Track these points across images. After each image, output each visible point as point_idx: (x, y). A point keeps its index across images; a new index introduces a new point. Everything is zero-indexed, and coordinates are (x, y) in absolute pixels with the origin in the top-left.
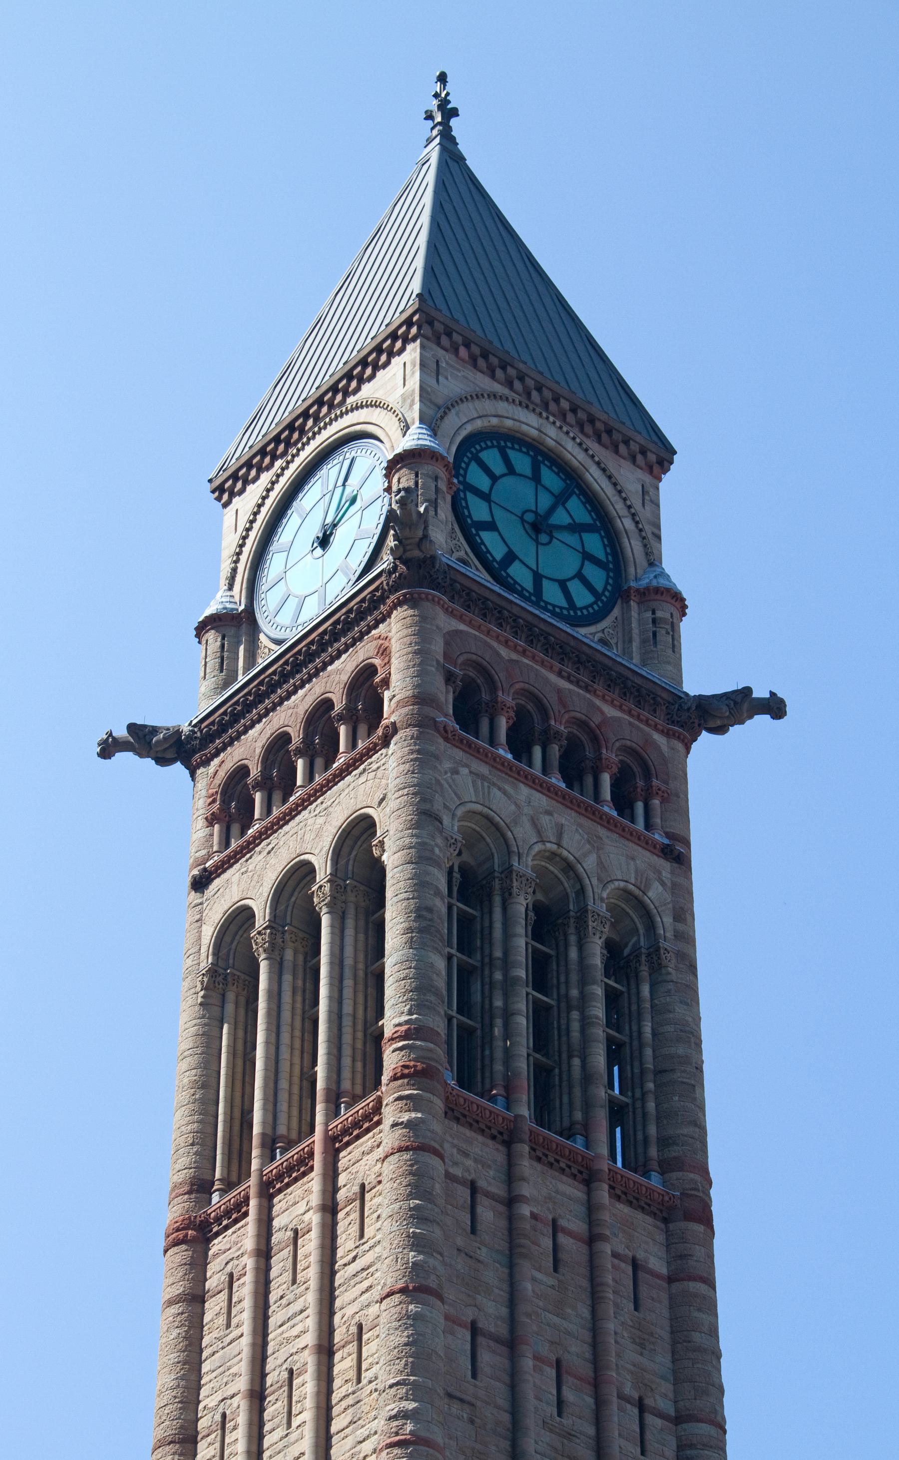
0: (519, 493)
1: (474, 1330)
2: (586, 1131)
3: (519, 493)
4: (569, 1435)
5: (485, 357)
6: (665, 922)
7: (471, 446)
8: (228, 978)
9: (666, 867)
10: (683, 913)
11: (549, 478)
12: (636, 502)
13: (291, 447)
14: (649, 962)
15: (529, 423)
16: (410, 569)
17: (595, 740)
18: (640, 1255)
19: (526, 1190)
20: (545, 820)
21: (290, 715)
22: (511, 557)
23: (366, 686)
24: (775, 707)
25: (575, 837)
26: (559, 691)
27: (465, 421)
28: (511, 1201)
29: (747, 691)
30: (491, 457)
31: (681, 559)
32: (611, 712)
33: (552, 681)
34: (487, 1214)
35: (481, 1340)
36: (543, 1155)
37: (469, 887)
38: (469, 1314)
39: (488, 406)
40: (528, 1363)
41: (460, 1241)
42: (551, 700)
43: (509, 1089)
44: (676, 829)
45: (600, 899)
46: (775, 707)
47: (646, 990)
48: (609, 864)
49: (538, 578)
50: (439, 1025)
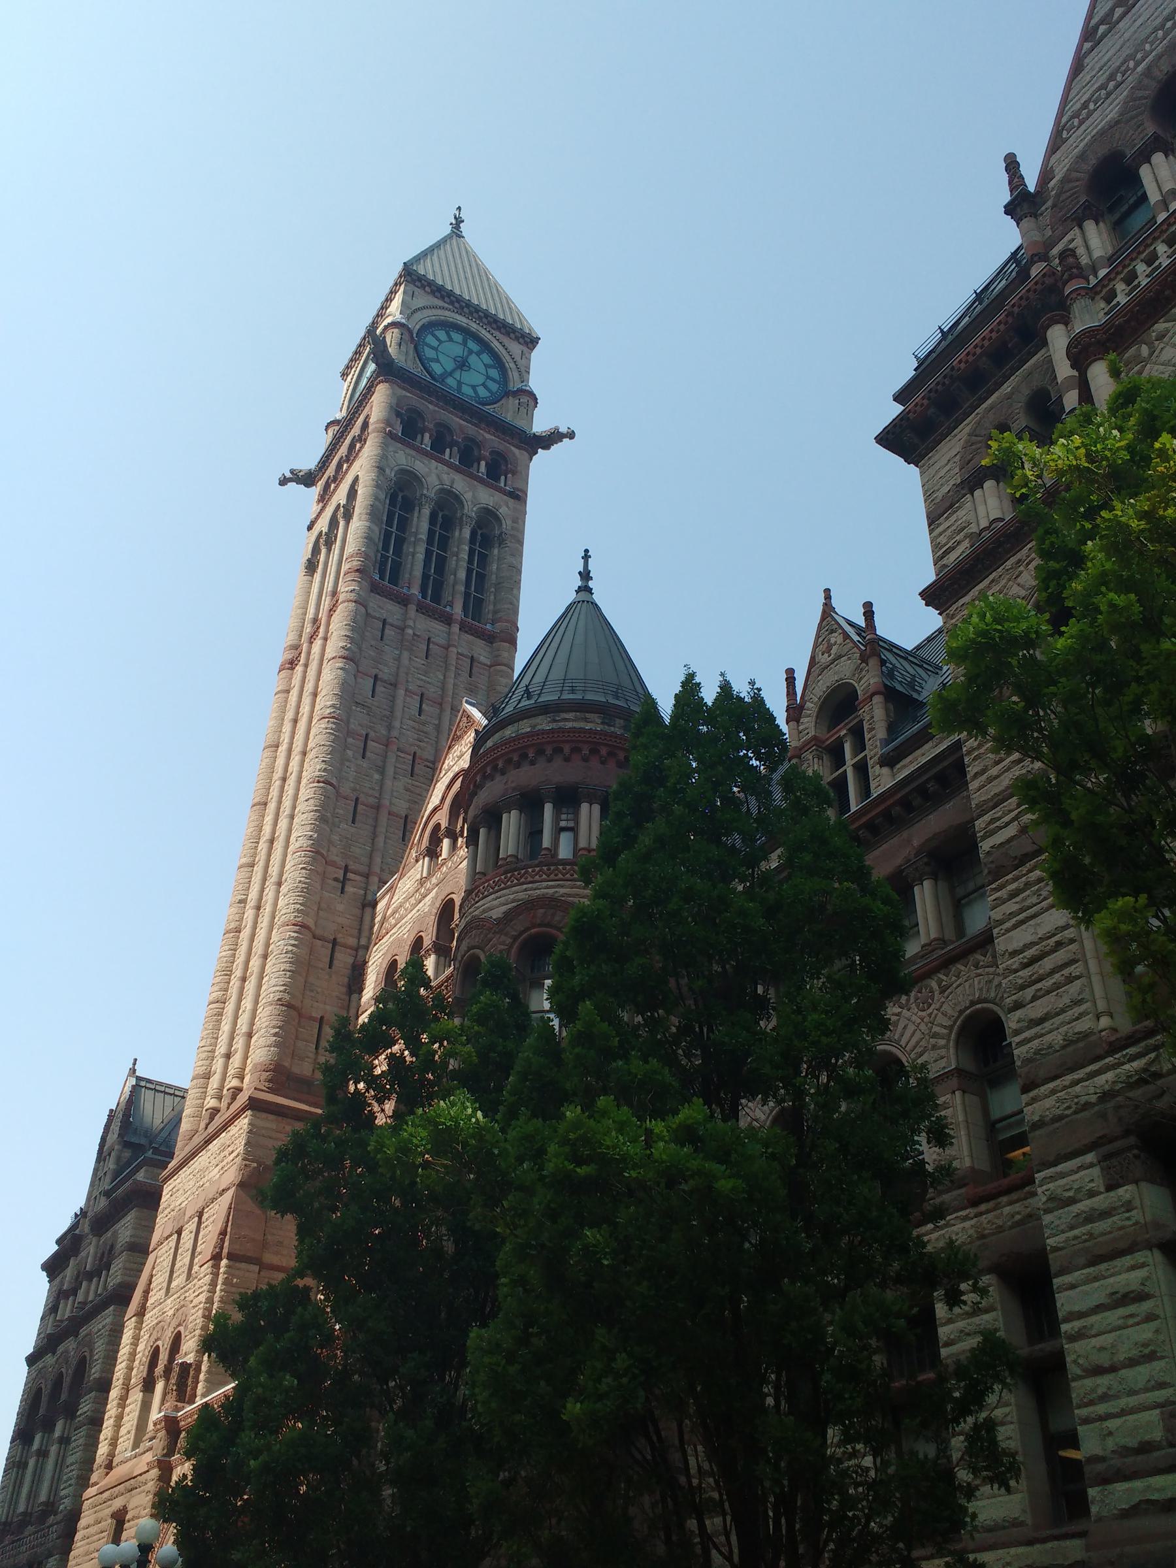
1: (376, 678)
4: (424, 724)
6: (507, 524)
9: (511, 502)
18: (475, 655)
20: (445, 477)
25: (460, 484)
26: (461, 425)
29: (557, 429)
31: (536, 382)
32: (488, 436)
34: (389, 632)
35: (379, 683)
36: (421, 609)
38: (374, 671)
40: (401, 692)
41: (373, 643)
44: (518, 485)
45: (470, 510)
47: (496, 551)
48: (476, 496)
50: (372, 555)
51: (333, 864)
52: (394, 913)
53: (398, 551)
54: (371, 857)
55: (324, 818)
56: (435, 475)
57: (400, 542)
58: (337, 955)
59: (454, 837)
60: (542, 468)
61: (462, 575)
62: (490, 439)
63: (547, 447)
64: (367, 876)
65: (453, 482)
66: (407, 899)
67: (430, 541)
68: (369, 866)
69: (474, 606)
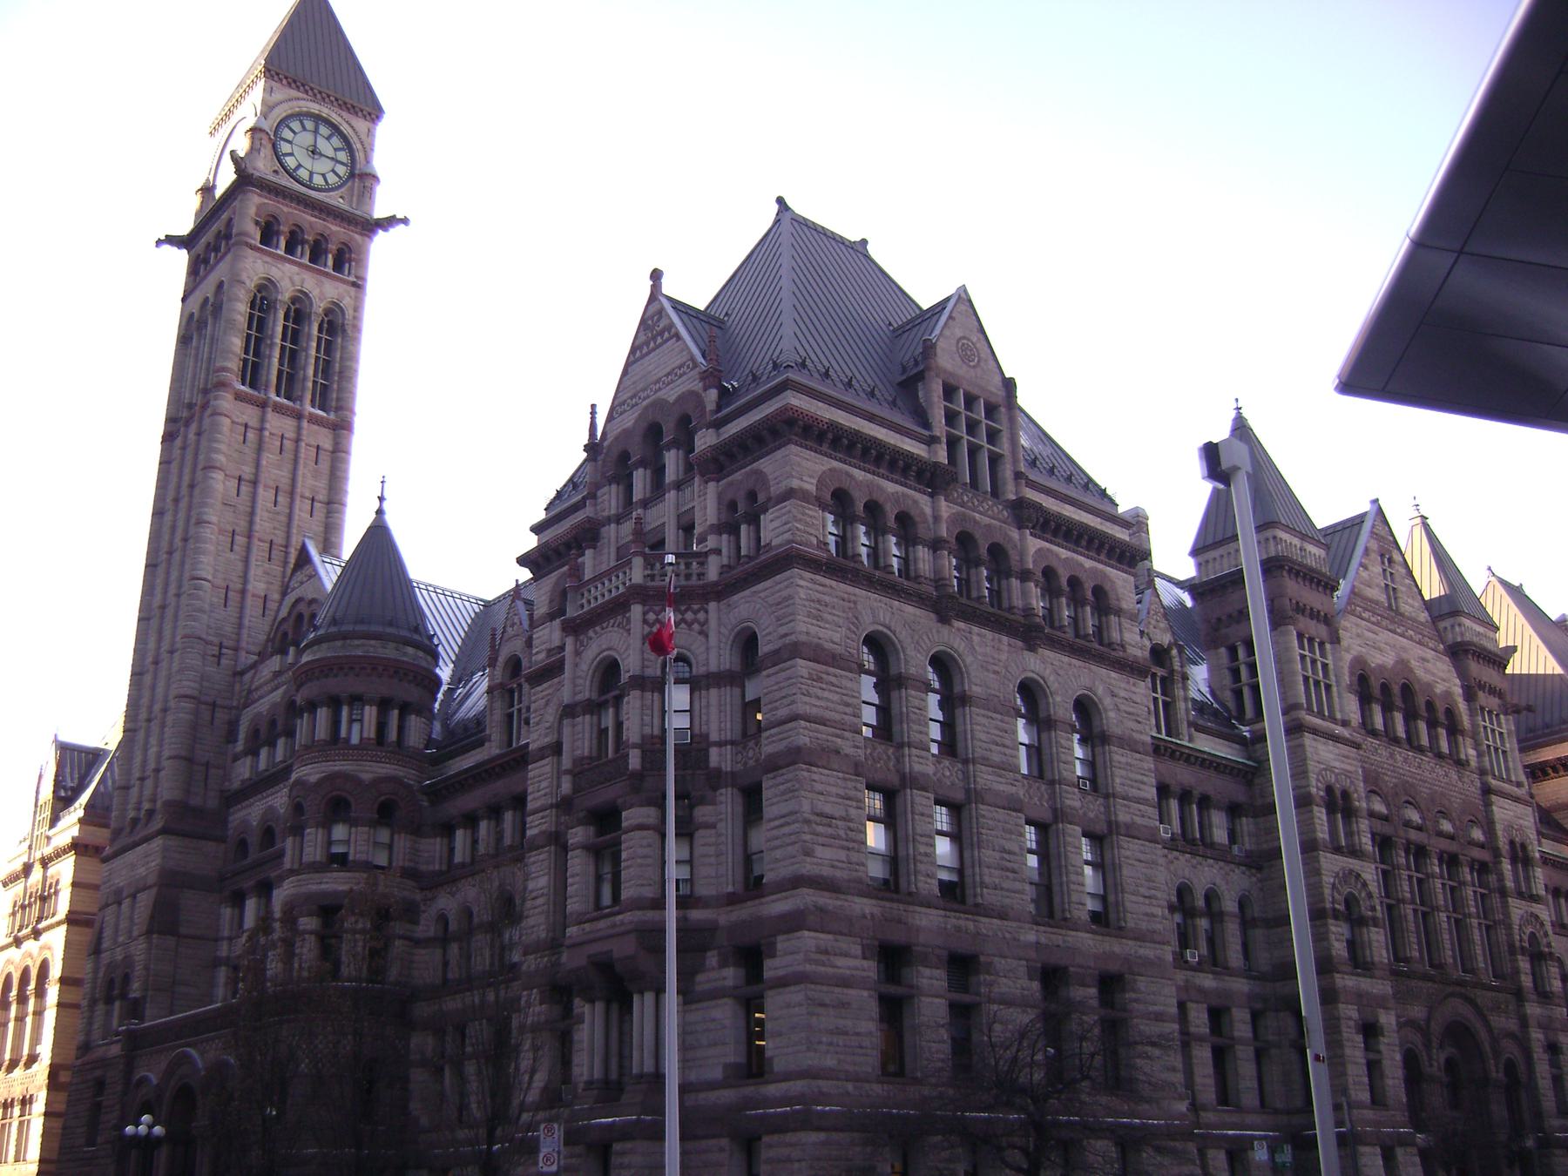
0: (306, 139)
1: (240, 479)
2: (301, 399)
5: (293, 83)
6: (349, 313)
7: (283, 122)
9: (352, 290)
10: (358, 308)
11: (324, 130)
12: (363, 137)
14: (338, 330)
17: (326, 240)
19: (267, 426)
20: (297, 279)
22: (300, 166)
24: (405, 221)
28: (262, 429)
30: (296, 125)
31: (381, 161)
32: (334, 228)
33: (308, 219)
34: (251, 435)
38: (237, 474)
39: (295, 103)
40: (261, 490)
42: (306, 226)
43: (267, 386)
45: (319, 307)
46: (405, 221)
48: (323, 291)
49: (311, 174)
51: (211, 643)
53: (257, 354)
54: (238, 634)
56: (290, 277)
57: (258, 341)
58: (217, 715)
60: (381, 251)
61: (311, 372)
62: (335, 229)
63: (386, 230)
64: (236, 649)
65: (303, 281)
66: (266, 683)
67: (284, 339)
68: (238, 641)
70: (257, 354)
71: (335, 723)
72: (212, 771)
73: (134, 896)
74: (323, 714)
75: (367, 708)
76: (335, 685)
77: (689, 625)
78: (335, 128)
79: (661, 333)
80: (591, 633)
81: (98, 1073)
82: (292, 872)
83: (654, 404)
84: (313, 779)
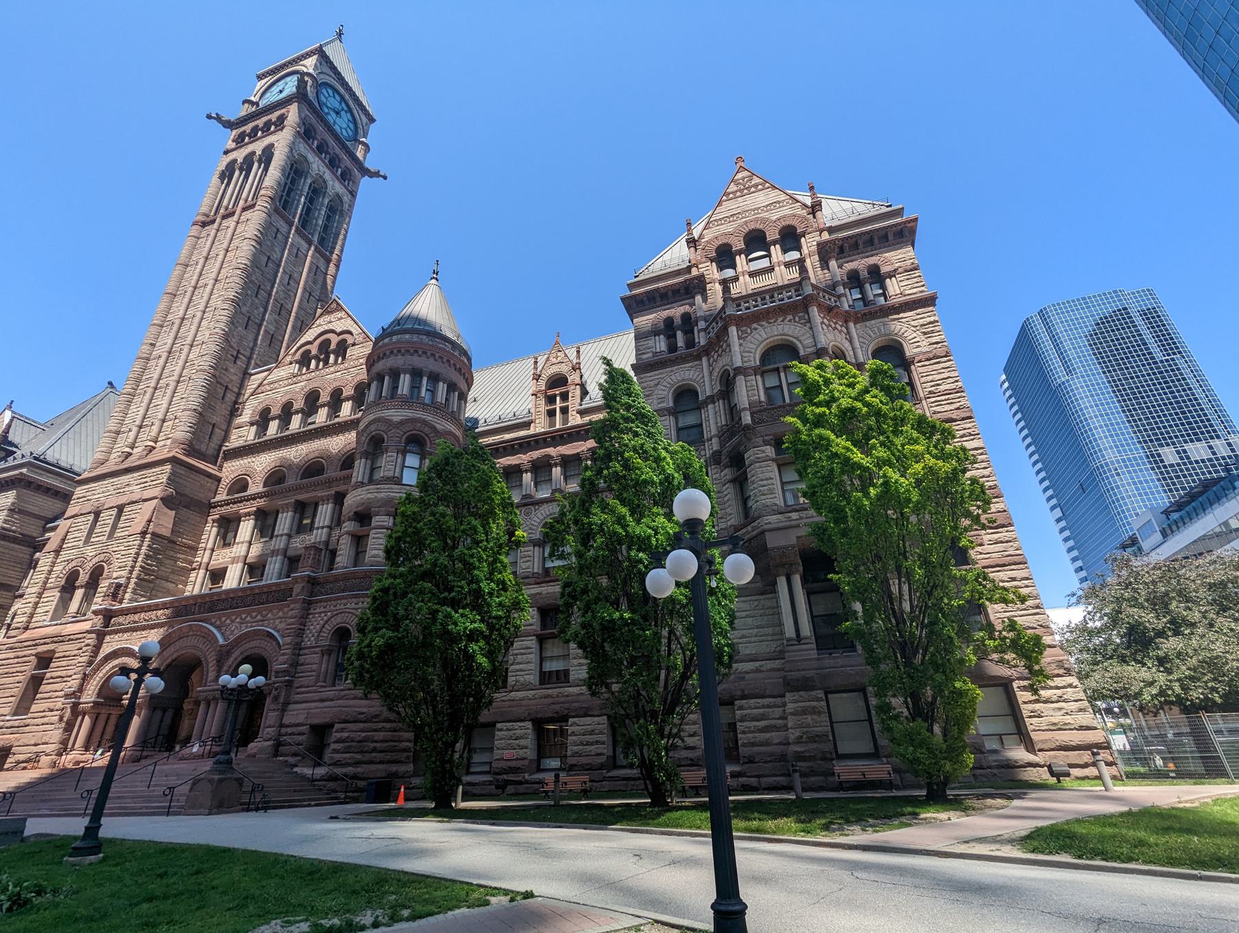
3: (334, 102)
6: (346, 206)
7: (326, 84)
8: (227, 175)
10: (351, 206)
13: (277, 73)
14: (338, 211)
15: (342, 91)
16: (300, 96)
21: (260, 122)
23: (282, 119)
25: (328, 175)
27: (323, 78)
30: (330, 92)
33: (331, 142)
34: (279, 236)
37: (295, 170)
45: (330, 191)
46: (385, 178)
48: (335, 187)
52: (270, 384)
53: (288, 195)
55: (232, 322)
56: (317, 165)
57: (290, 190)
59: (318, 360)
69: (322, 241)
70: (288, 195)
71: (415, 387)
72: (217, 430)
73: (120, 509)
74: (405, 381)
75: (441, 384)
76: (417, 361)
77: (840, 332)
78: (350, 110)
79: (756, 186)
80: (755, 325)
81: (41, 649)
82: (362, 484)
83: (756, 220)
84: (396, 419)
